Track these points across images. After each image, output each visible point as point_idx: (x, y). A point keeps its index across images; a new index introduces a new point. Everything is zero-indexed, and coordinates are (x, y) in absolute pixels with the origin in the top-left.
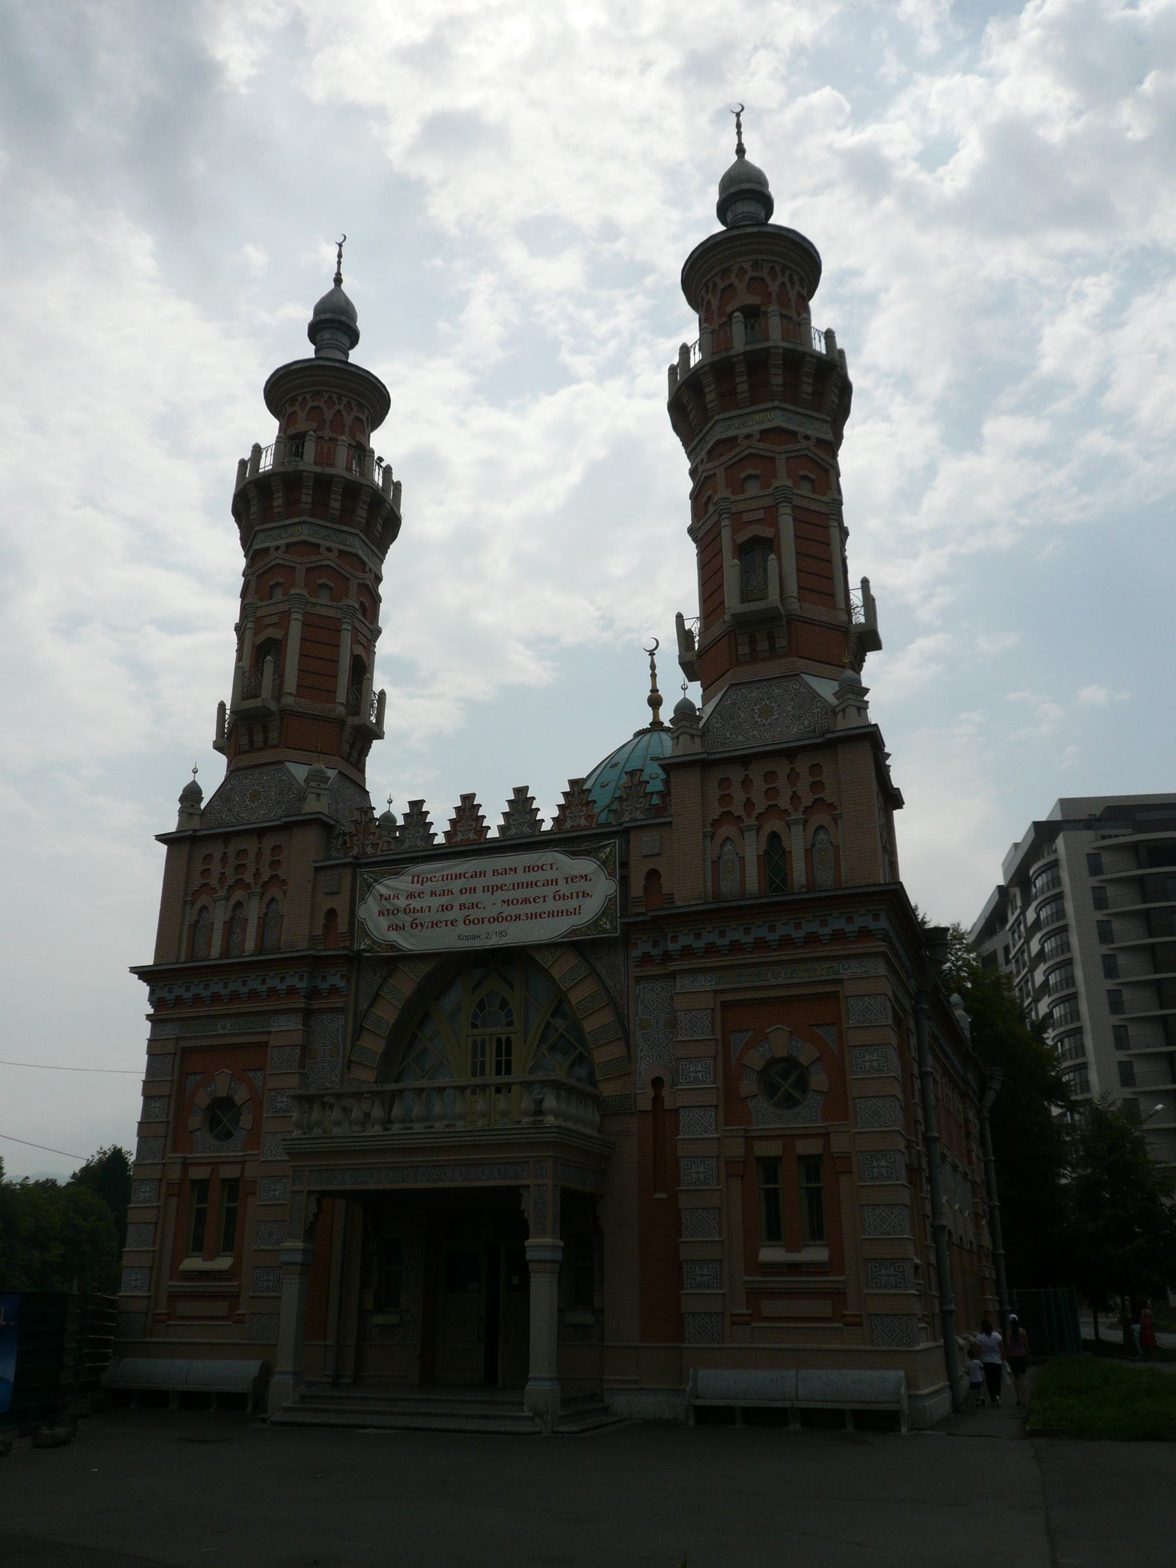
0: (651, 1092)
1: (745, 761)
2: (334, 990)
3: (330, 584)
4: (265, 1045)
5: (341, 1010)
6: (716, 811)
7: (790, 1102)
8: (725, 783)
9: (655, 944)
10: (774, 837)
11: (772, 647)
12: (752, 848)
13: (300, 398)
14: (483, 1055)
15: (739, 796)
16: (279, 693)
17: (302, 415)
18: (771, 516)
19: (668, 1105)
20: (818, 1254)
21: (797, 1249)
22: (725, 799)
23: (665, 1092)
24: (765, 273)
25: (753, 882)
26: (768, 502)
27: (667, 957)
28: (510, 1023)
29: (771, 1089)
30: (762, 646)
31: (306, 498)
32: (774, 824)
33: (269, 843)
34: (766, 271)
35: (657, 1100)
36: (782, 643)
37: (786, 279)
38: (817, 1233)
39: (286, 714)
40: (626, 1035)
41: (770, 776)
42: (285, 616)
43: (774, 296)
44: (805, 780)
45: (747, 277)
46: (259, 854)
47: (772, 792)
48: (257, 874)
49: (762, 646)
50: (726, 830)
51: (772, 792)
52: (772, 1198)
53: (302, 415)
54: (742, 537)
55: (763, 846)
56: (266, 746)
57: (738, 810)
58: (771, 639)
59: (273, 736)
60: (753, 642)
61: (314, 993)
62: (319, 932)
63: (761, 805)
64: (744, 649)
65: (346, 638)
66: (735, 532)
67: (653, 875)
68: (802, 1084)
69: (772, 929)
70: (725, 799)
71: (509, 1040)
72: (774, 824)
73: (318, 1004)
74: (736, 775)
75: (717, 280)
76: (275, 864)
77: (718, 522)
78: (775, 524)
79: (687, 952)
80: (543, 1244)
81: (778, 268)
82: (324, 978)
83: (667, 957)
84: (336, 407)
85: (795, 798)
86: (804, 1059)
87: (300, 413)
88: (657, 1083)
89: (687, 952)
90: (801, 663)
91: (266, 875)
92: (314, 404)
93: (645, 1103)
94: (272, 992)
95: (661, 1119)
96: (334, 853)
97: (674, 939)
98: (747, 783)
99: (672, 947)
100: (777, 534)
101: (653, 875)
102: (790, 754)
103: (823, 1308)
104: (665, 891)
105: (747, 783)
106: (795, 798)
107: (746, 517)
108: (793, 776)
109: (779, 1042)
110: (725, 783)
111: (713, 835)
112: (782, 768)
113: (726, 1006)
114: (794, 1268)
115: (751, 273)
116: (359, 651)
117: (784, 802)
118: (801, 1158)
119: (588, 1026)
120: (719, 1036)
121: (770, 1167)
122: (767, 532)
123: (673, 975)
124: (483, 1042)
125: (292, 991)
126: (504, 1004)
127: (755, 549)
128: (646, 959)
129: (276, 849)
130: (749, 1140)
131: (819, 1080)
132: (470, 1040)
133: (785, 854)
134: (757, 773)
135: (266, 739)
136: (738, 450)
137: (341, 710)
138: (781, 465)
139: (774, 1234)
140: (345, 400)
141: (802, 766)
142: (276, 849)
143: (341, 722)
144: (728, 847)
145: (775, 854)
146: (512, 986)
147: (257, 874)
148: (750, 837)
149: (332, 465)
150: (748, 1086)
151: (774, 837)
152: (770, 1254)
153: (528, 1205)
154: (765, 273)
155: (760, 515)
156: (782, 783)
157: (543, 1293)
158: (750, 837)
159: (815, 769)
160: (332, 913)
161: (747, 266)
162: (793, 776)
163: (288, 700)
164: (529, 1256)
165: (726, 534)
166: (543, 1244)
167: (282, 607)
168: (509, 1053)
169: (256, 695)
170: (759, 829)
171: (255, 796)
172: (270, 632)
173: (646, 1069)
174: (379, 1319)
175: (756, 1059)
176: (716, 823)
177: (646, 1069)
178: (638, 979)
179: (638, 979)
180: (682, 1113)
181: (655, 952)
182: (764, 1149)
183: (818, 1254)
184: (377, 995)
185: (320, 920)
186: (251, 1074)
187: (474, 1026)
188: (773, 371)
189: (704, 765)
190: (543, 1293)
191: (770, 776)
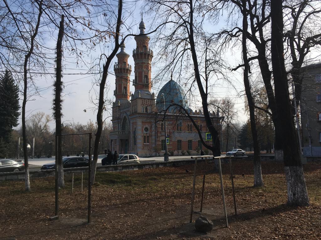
1: (145, 99)
6: (142, 103)
22: (143, 102)
38: (148, 142)
44: (149, 101)
47: (147, 103)
51: (147, 103)
54: (145, 75)
63: (146, 104)
70: (143, 102)
102: (148, 99)
109: (147, 126)
110: (143, 101)
112: (148, 100)
121: (145, 136)
134: (145, 100)
141: (149, 100)
152: (145, 144)
175: (145, 127)
176: (141, 104)
182: (144, 135)
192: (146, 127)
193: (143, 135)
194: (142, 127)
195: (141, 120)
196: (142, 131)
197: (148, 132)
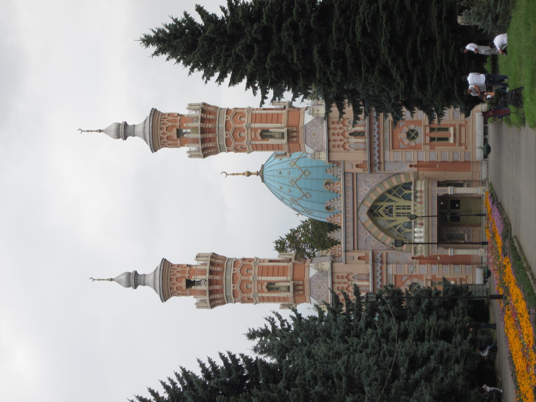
0: (413, 168)
1: (329, 141)
2: (381, 256)
3: (246, 269)
4: (395, 276)
5: (387, 254)
7: (417, 134)
8: (334, 146)
9: (376, 166)
10: (351, 134)
11: (295, 132)
12: (353, 140)
13: (171, 286)
14: (400, 213)
15: (338, 143)
16: (287, 281)
17: (179, 284)
18: (254, 130)
19: (416, 164)
20: (451, 130)
21: (450, 134)
22: (338, 146)
23: (413, 164)
24: (165, 126)
25: (361, 140)
26: (249, 130)
27: (379, 163)
28: (392, 206)
29: (413, 138)
30: (295, 134)
31: (217, 278)
32: (347, 134)
33: (336, 280)
34: (163, 126)
35: (415, 166)
36: (295, 129)
37: (166, 120)
38: (447, 129)
39: (293, 279)
40: (398, 174)
41: (333, 134)
42: (259, 282)
43: (173, 124)
45: (166, 132)
46: (339, 283)
48: (345, 283)
49: (295, 134)
50: (347, 146)
52: (439, 139)
53: (179, 284)
54: (260, 138)
55: (352, 137)
56: (303, 285)
57: (342, 143)
58: (293, 132)
59: (300, 283)
60: (293, 137)
61: (382, 262)
62: (364, 262)
63: (342, 137)
64: (295, 139)
65: (264, 264)
66: (257, 140)
67: (357, 166)
68: (413, 131)
69: (375, 136)
70: (338, 146)
71: (397, 206)
72: (347, 134)
73: (385, 261)
74: (332, 143)
75: (162, 141)
76: (342, 277)
77: (252, 145)
78: (256, 129)
79: (379, 157)
80: (450, 190)
81: (162, 122)
82: (378, 259)
83: (379, 163)
84: (176, 273)
85: (340, 128)
86: (407, 130)
87: (178, 285)
88: (411, 166)
89: (379, 157)
90: (301, 124)
91: (346, 280)
92: (175, 280)
93: (415, 169)
94: (381, 274)
95: (420, 165)
96: (340, 260)
97: (375, 161)
98: (335, 141)
99: (377, 161)
100: (260, 128)
101: (357, 166)
102: (329, 129)
103: (463, 129)
104: (362, 163)
105: (335, 141)
106: (340, 128)
107: (253, 136)
108: (334, 129)
109: (402, 135)
110: (334, 146)
111: (348, 150)
112: (332, 131)
113: (393, 149)
114: (455, 135)
115: (165, 130)
116: (267, 261)
117: (342, 131)
118: (430, 132)
119: (395, 184)
120: (400, 150)
121: (432, 139)
122: (259, 131)
123: (384, 161)
124: (397, 213)
125: (381, 268)
126: (387, 208)
127: (265, 134)
128: (379, 168)
129: (338, 277)
130: (425, 144)
131: (412, 127)
132: (397, 217)
133: (355, 132)
134: (332, 138)
135: (301, 285)
136: (231, 138)
137: (290, 264)
138: (238, 126)
139: (447, 139)
140: (172, 270)
142: (338, 277)
143: (294, 264)
144: (352, 146)
145: (355, 134)
146: (382, 206)
147: (345, 283)
148: (350, 140)
149: (205, 270)
150: (413, 143)
151: (351, 134)
152: (451, 140)
153: (441, 194)
154: (165, 126)
155: (253, 133)
156: (336, 132)
157: (460, 191)
158: (350, 140)
159: (333, 123)
160: (359, 258)
161: (162, 132)
162: (334, 129)
163: (289, 278)
164: (452, 193)
165: (257, 143)
166: (450, 190)
167: (256, 283)
168: (400, 206)
169: (289, 287)
170: (348, 138)
171: (319, 287)
172: (264, 287)
173: (407, 169)
174: (466, 239)
175: (406, 141)
177: (407, 169)
178: (384, 170)
179: (384, 170)
180: (419, 160)
181: (378, 166)
182: (428, 140)
183: (451, 130)
184: (383, 243)
185: (361, 261)
186: (403, 280)
187: (392, 216)
188: (207, 126)
189: (329, 151)
190: (460, 191)
191: (333, 134)
192: (405, 135)
193: (428, 147)
194: (410, 148)
195: (387, 153)
196: (417, 148)
197: (421, 130)
